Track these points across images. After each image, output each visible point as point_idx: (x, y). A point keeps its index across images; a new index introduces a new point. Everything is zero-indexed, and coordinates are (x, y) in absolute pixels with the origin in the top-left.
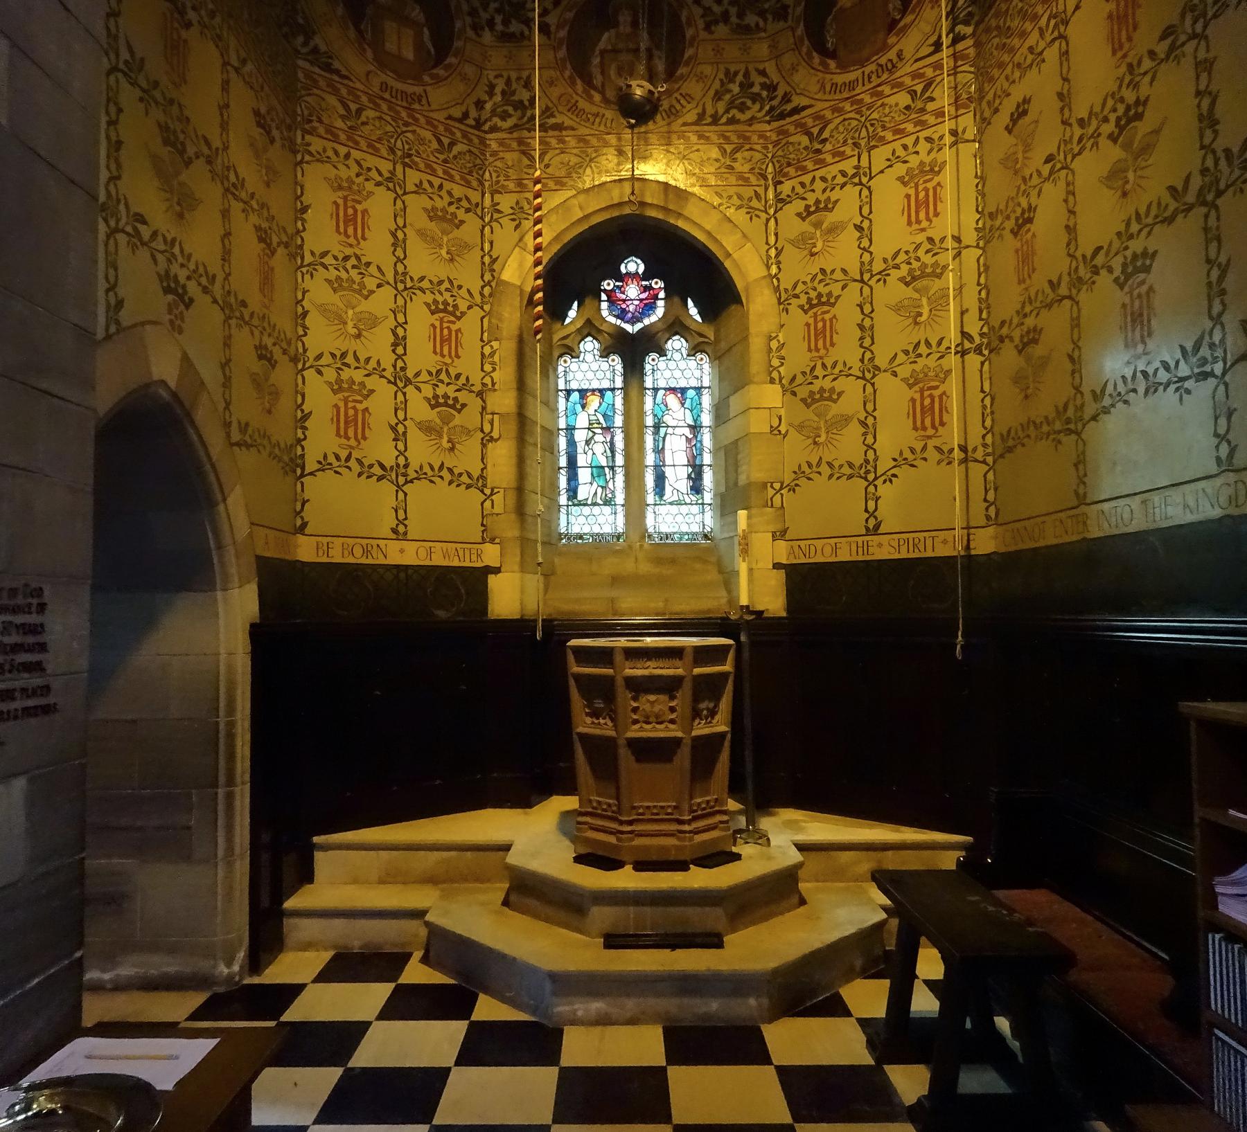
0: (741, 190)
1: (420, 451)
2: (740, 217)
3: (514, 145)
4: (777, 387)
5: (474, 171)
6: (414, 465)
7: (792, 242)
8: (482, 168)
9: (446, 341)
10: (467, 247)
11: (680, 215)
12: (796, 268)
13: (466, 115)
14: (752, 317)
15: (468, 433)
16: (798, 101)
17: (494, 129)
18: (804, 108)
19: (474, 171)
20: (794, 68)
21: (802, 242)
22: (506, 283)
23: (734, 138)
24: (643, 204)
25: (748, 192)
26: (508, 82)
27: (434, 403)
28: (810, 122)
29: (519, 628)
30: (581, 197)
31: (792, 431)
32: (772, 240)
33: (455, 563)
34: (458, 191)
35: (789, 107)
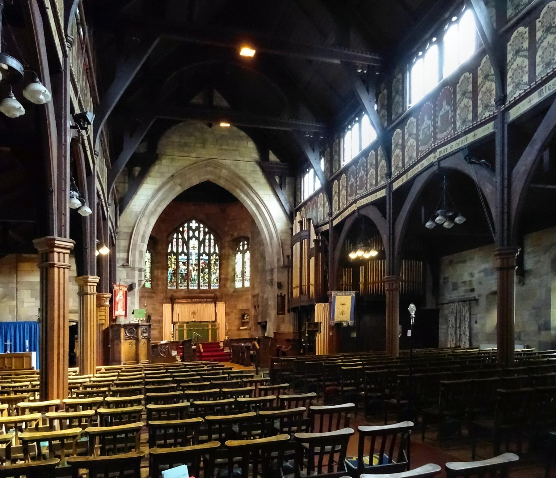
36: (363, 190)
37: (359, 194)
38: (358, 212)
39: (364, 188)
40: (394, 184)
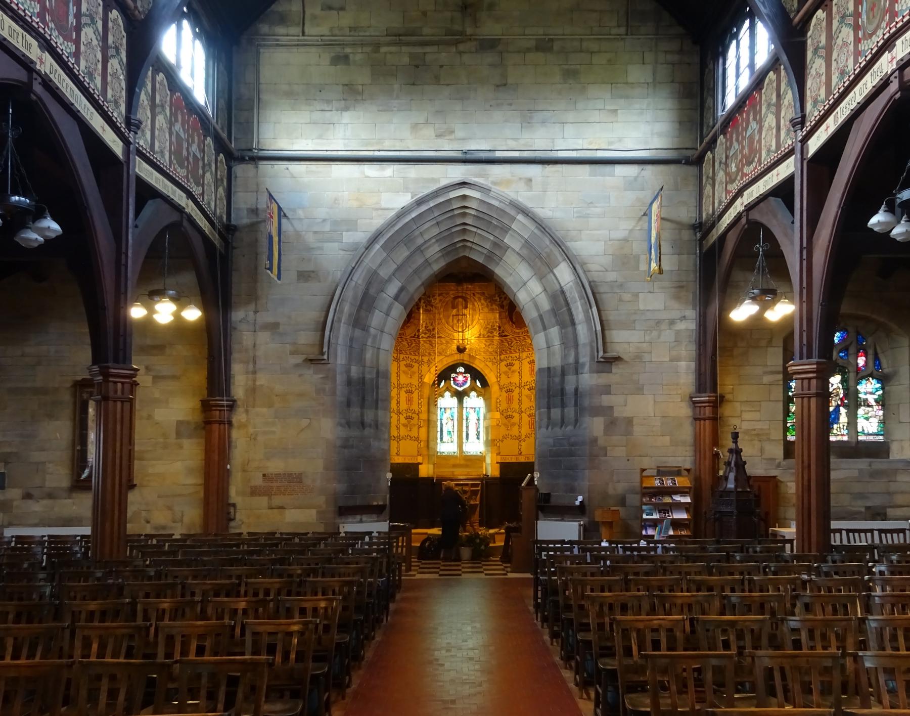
0: (490, 357)
1: (403, 432)
2: (490, 364)
3: (428, 342)
4: (499, 413)
5: (417, 351)
6: (401, 436)
7: (504, 372)
8: (419, 349)
9: (409, 401)
10: (414, 373)
11: (473, 363)
12: (504, 380)
13: (415, 335)
14: (492, 393)
15: (414, 425)
16: (506, 333)
17: (423, 337)
18: (507, 336)
19: (417, 351)
20: (505, 324)
21: (506, 373)
22: (425, 383)
23: (489, 341)
24: (463, 360)
25: (492, 357)
26: (426, 324)
27: (407, 418)
28: (508, 340)
29: (429, 480)
30: (446, 358)
31: (502, 426)
32: (498, 371)
33: (411, 462)
34: (413, 357)
35: (503, 334)
36: (754, 164)
37: (746, 175)
38: (747, 216)
39: (756, 160)
40: (809, 142)
